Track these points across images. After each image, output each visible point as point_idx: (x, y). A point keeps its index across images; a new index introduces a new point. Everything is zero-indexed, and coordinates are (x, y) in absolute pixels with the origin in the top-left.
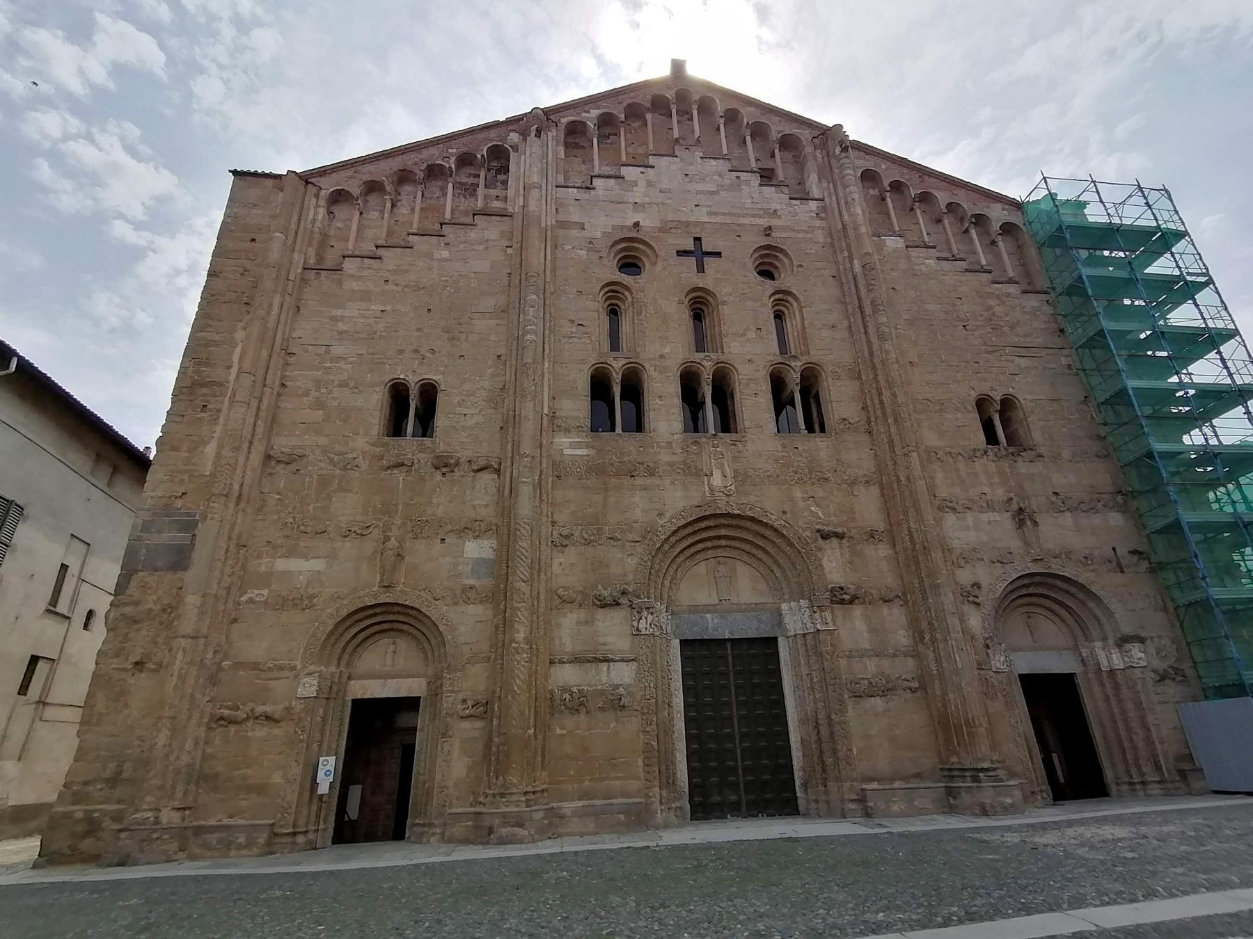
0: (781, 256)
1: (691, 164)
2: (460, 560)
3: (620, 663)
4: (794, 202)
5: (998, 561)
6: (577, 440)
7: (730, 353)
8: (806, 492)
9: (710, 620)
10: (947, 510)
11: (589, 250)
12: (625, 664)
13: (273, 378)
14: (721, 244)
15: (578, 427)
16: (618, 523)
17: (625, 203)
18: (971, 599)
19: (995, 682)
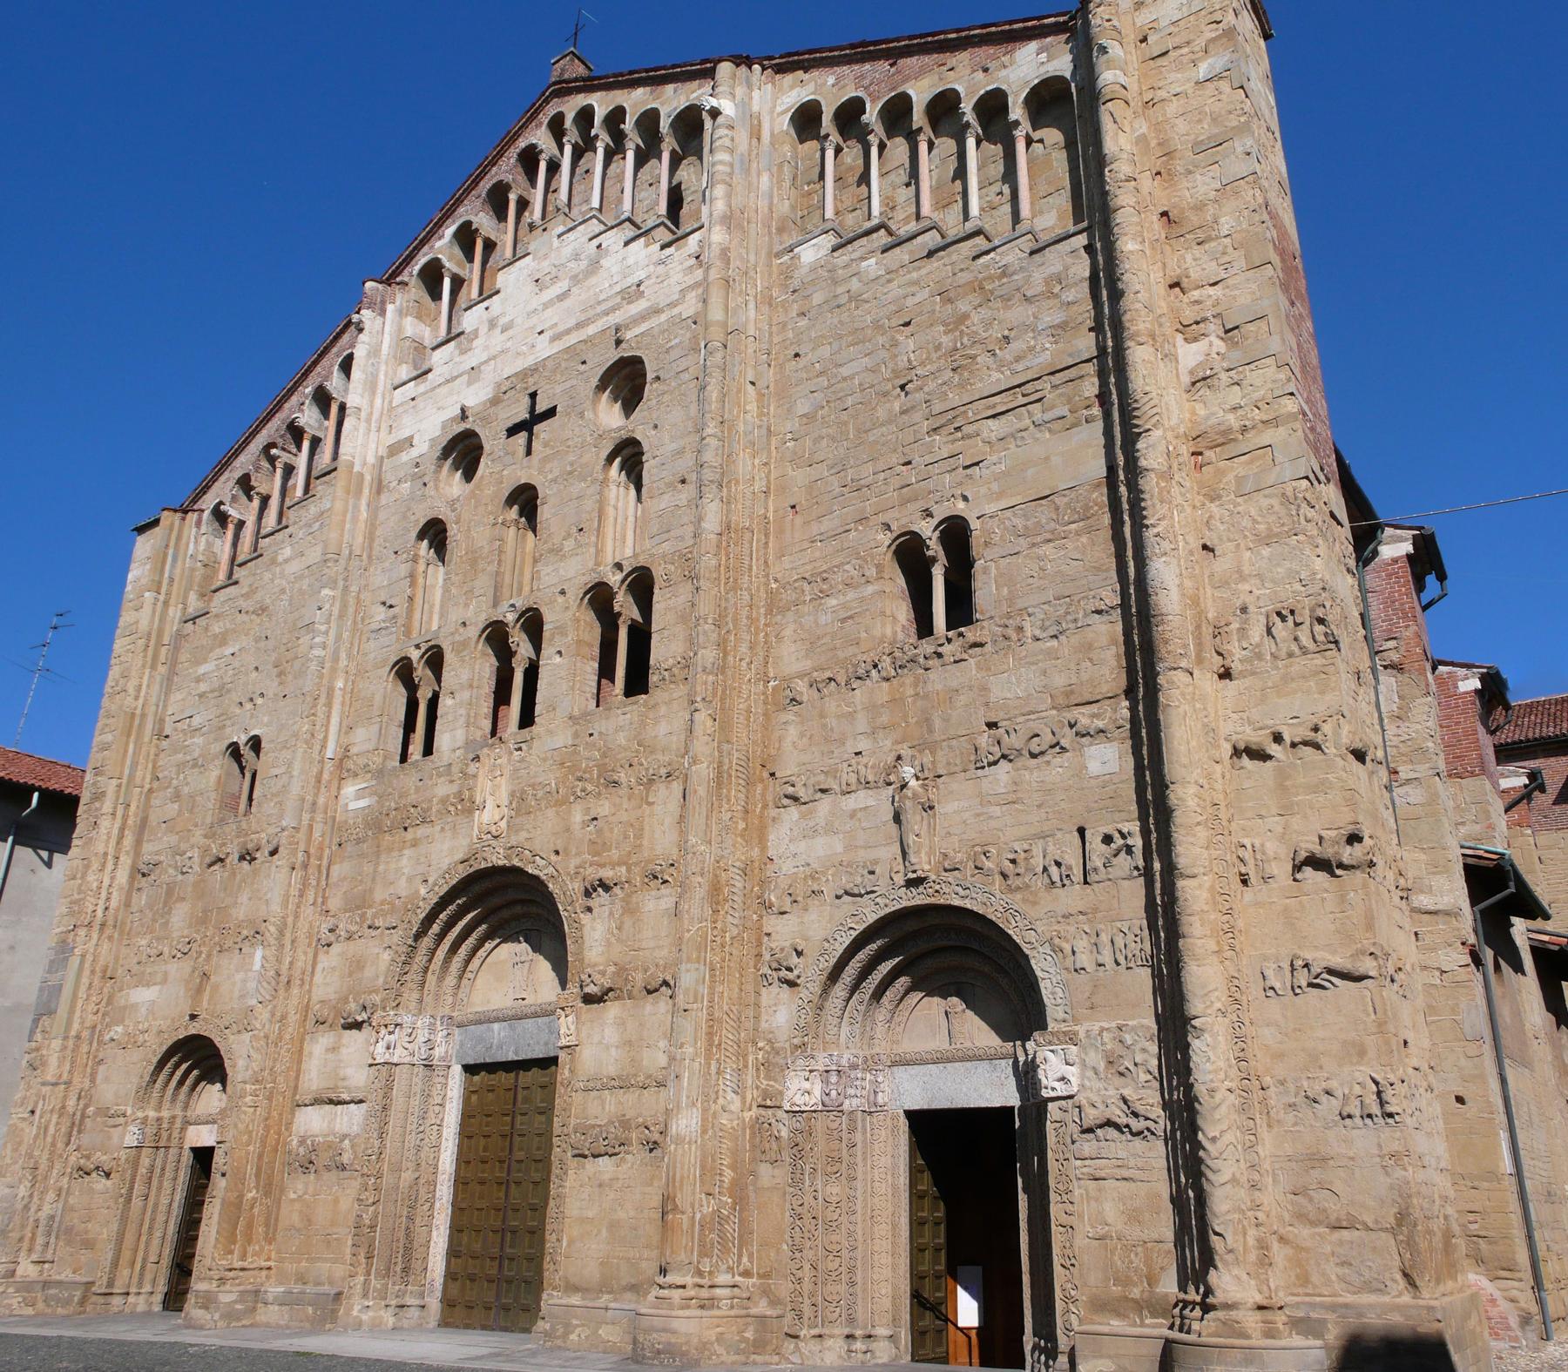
2: (250, 974)
5: (847, 893)
18: (784, 973)
19: (784, 1133)
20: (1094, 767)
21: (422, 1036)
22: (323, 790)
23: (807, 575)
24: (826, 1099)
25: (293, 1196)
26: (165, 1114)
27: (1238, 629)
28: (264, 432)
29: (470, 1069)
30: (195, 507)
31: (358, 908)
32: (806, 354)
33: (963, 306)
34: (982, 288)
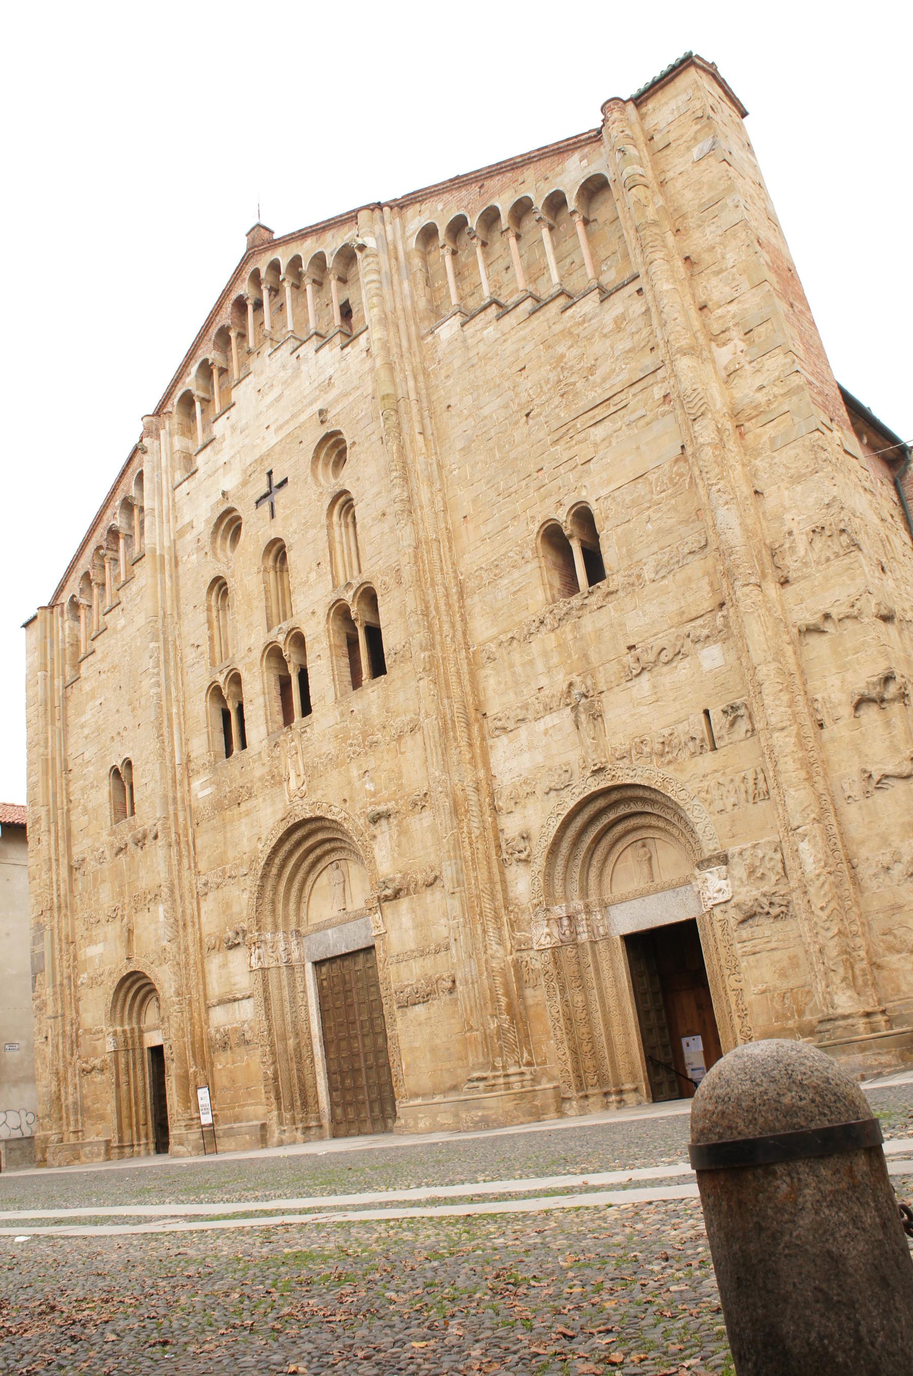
10: (497, 733)
13: (61, 799)
20: (707, 665)
21: (281, 946)
22: (178, 787)
23: (483, 566)
24: (563, 937)
25: (219, 1067)
26: (127, 1027)
27: (790, 548)
28: (94, 540)
29: (318, 964)
30: (58, 602)
31: (219, 865)
32: (456, 405)
33: (561, 349)
34: (570, 333)
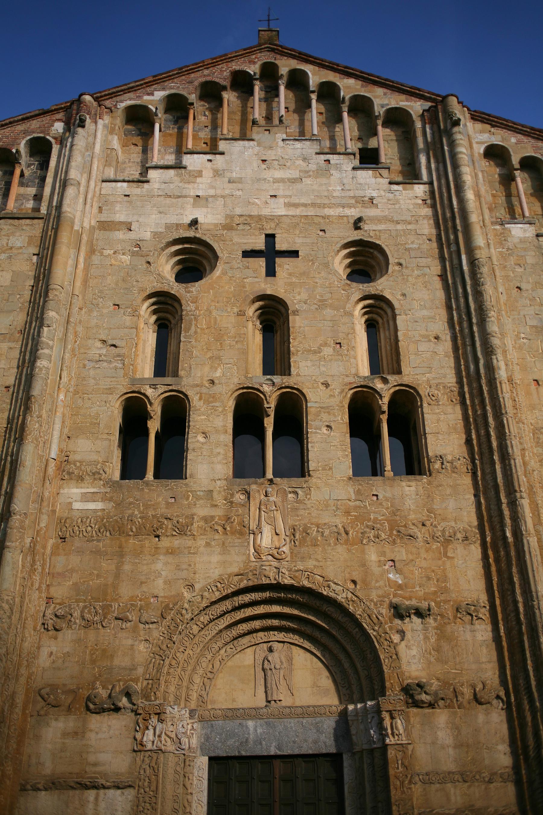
0: (376, 253)
1: (271, 148)
3: (111, 792)
4: (395, 187)
6: (92, 490)
7: (298, 375)
8: (384, 554)
9: (252, 729)
11: (133, 254)
12: (119, 792)
14: (299, 240)
15: (94, 474)
16: (132, 598)
17: (185, 197)
